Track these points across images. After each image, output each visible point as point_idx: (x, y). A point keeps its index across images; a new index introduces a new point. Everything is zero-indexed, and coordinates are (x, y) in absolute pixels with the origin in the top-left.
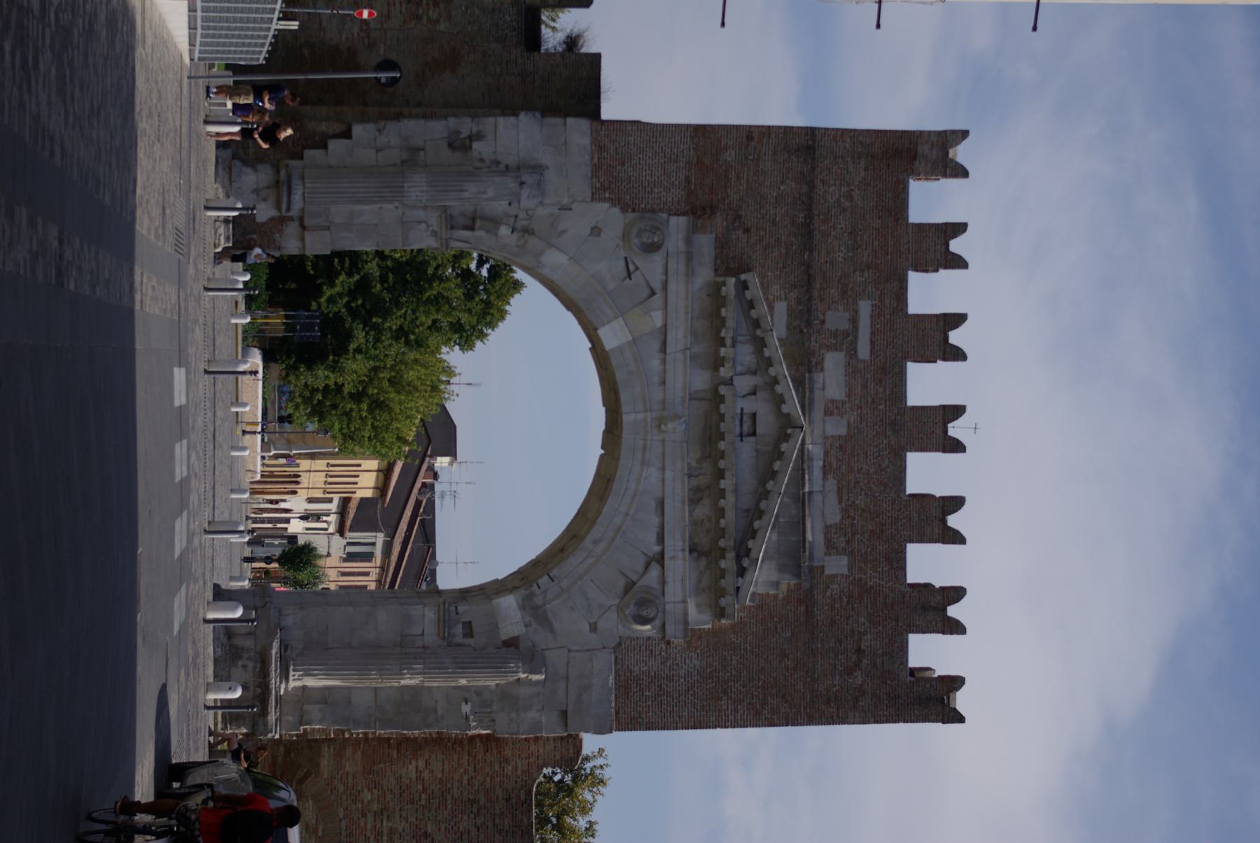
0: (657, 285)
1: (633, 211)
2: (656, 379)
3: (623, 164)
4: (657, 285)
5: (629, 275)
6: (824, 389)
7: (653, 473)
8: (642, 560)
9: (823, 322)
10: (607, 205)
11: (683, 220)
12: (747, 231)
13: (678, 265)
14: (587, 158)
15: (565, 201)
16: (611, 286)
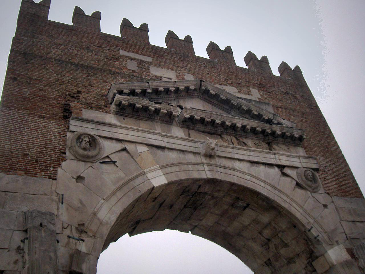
0: (119, 146)
1: (65, 153)
2: (181, 155)
3: (26, 155)
4: (119, 146)
5: (114, 162)
6: (171, 79)
7: (238, 165)
8: (284, 178)
9: (134, 71)
10: (60, 170)
11: (72, 122)
12: (79, 92)
13: (105, 132)
14: (20, 178)
15: (55, 198)
16: (122, 174)
